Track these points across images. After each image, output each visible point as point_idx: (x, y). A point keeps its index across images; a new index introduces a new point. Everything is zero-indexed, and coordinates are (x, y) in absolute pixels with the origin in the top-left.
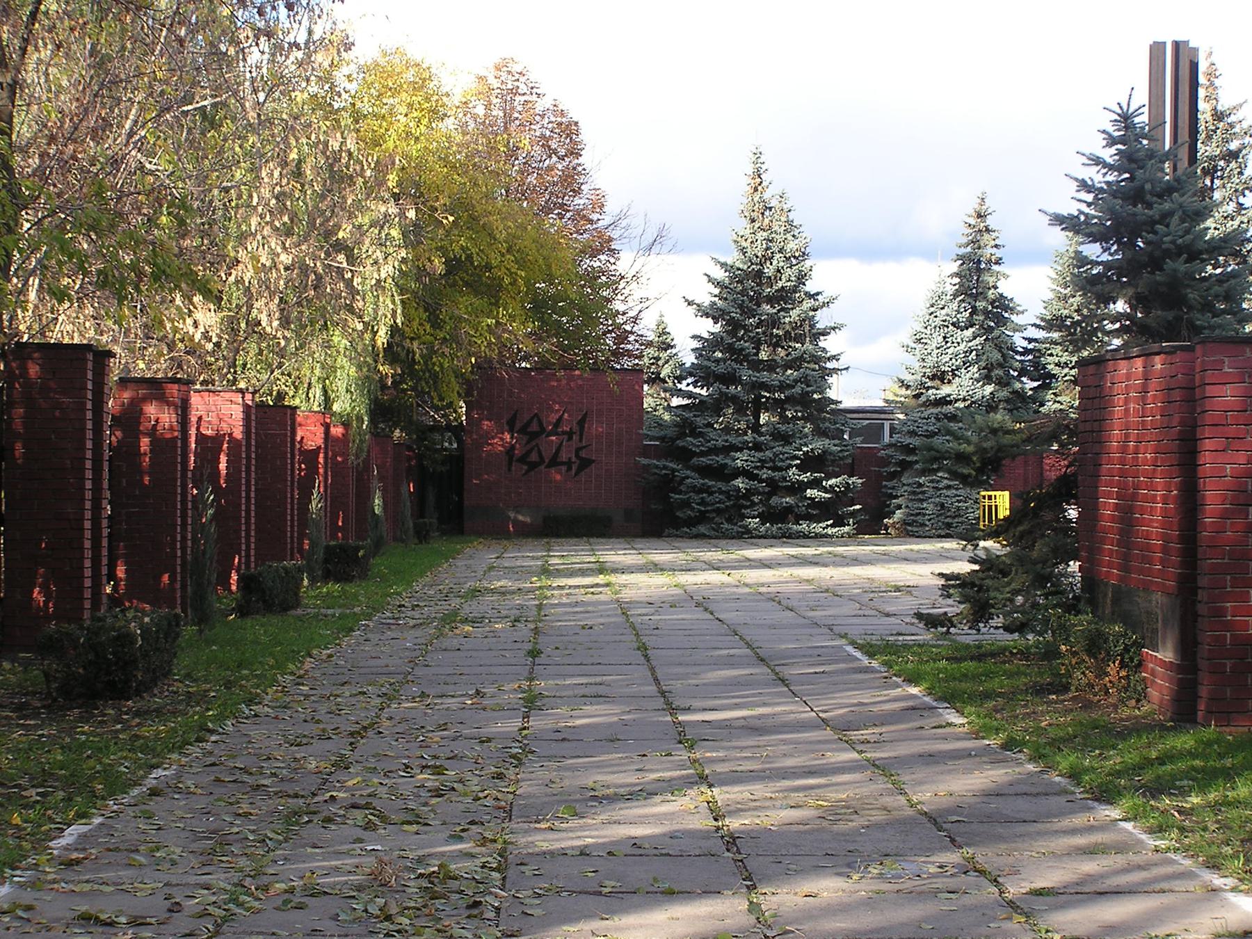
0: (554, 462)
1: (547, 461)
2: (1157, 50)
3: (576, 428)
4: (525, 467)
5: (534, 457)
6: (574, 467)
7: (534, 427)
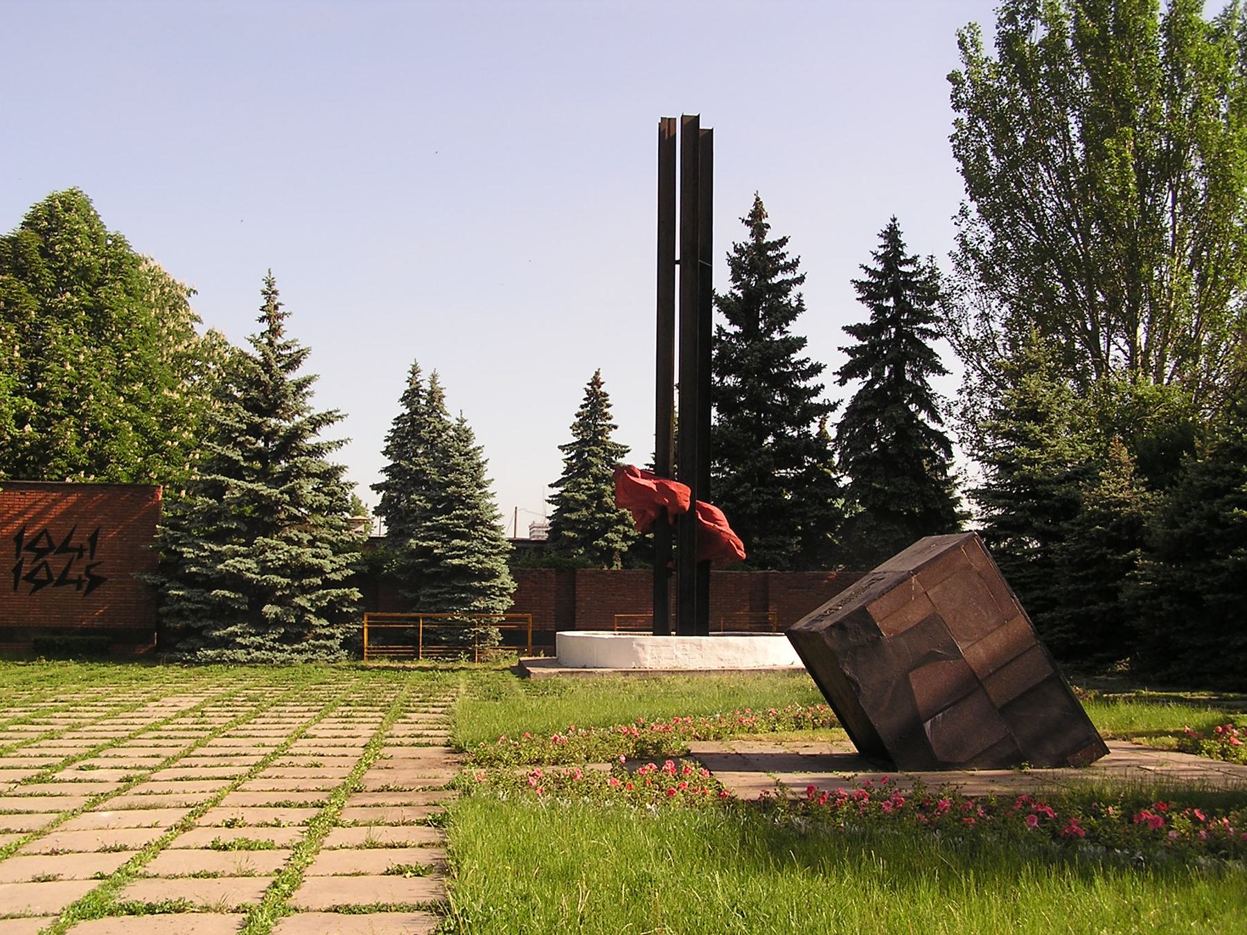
0: (63, 581)
1: (56, 579)
2: (666, 127)
3: (87, 545)
4: (33, 585)
5: (42, 575)
6: (85, 586)
7: (43, 544)
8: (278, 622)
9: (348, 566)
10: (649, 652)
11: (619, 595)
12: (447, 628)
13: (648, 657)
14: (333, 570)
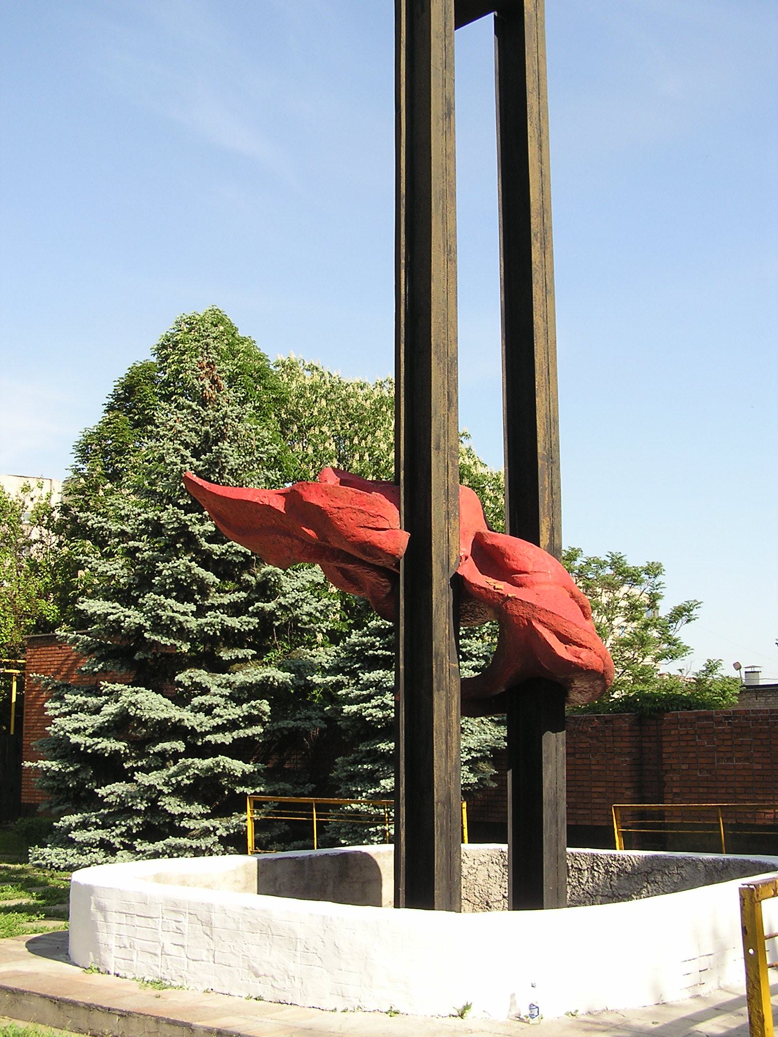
8: (124, 810)
9: (251, 720)
10: (115, 928)
11: (739, 759)
12: (354, 825)
13: (113, 942)
14: (217, 729)
